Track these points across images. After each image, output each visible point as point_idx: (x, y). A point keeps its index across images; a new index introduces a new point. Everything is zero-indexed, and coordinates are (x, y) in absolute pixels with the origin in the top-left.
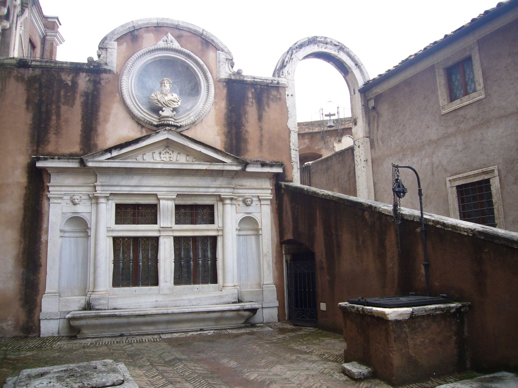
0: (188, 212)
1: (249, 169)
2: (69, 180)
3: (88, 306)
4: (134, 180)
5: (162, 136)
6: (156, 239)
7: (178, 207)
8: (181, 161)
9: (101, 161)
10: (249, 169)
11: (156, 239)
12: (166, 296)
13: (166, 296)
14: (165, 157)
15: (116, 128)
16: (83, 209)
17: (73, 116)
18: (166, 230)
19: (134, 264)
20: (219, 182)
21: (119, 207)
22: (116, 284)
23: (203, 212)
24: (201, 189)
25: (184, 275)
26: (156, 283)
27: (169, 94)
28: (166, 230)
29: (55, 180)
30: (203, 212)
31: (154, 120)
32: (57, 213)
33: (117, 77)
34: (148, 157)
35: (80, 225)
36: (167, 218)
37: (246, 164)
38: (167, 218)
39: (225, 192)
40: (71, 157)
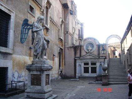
0: (93, 64)
1: (100, 58)
2: (79, 60)
3: (81, 75)
4: (86, 60)
5: (88, 54)
6: (88, 67)
7: (91, 63)
8: (91, 57)
9: (82, 58)
10: (100, 58)
11: (88, 67)
12: (90, 74)
13: (90, 74)
14: (89, 57)
15: (83, 53)
16: (80, 64)
17: (78, 51)
18: (90, 66)
19: (86, 70)
20: (97, 59)
21: (84, 63)
22: (84, 73)
23: (95, 64)
24: (94, 61)
25: (92, 72)
26: (89, 73)
27: (90, 48)
28: (90, 66)
29: (77, 60)
30: (95, 64)
31: (88, 52)
32: (77, 64)
33: (83, 46)
34: (87, 57)
35: (80, 65)
36: (90, 65)
37: (99, 57)
38: (90, 65)
39: (97, 61)
40: (78, 57)
